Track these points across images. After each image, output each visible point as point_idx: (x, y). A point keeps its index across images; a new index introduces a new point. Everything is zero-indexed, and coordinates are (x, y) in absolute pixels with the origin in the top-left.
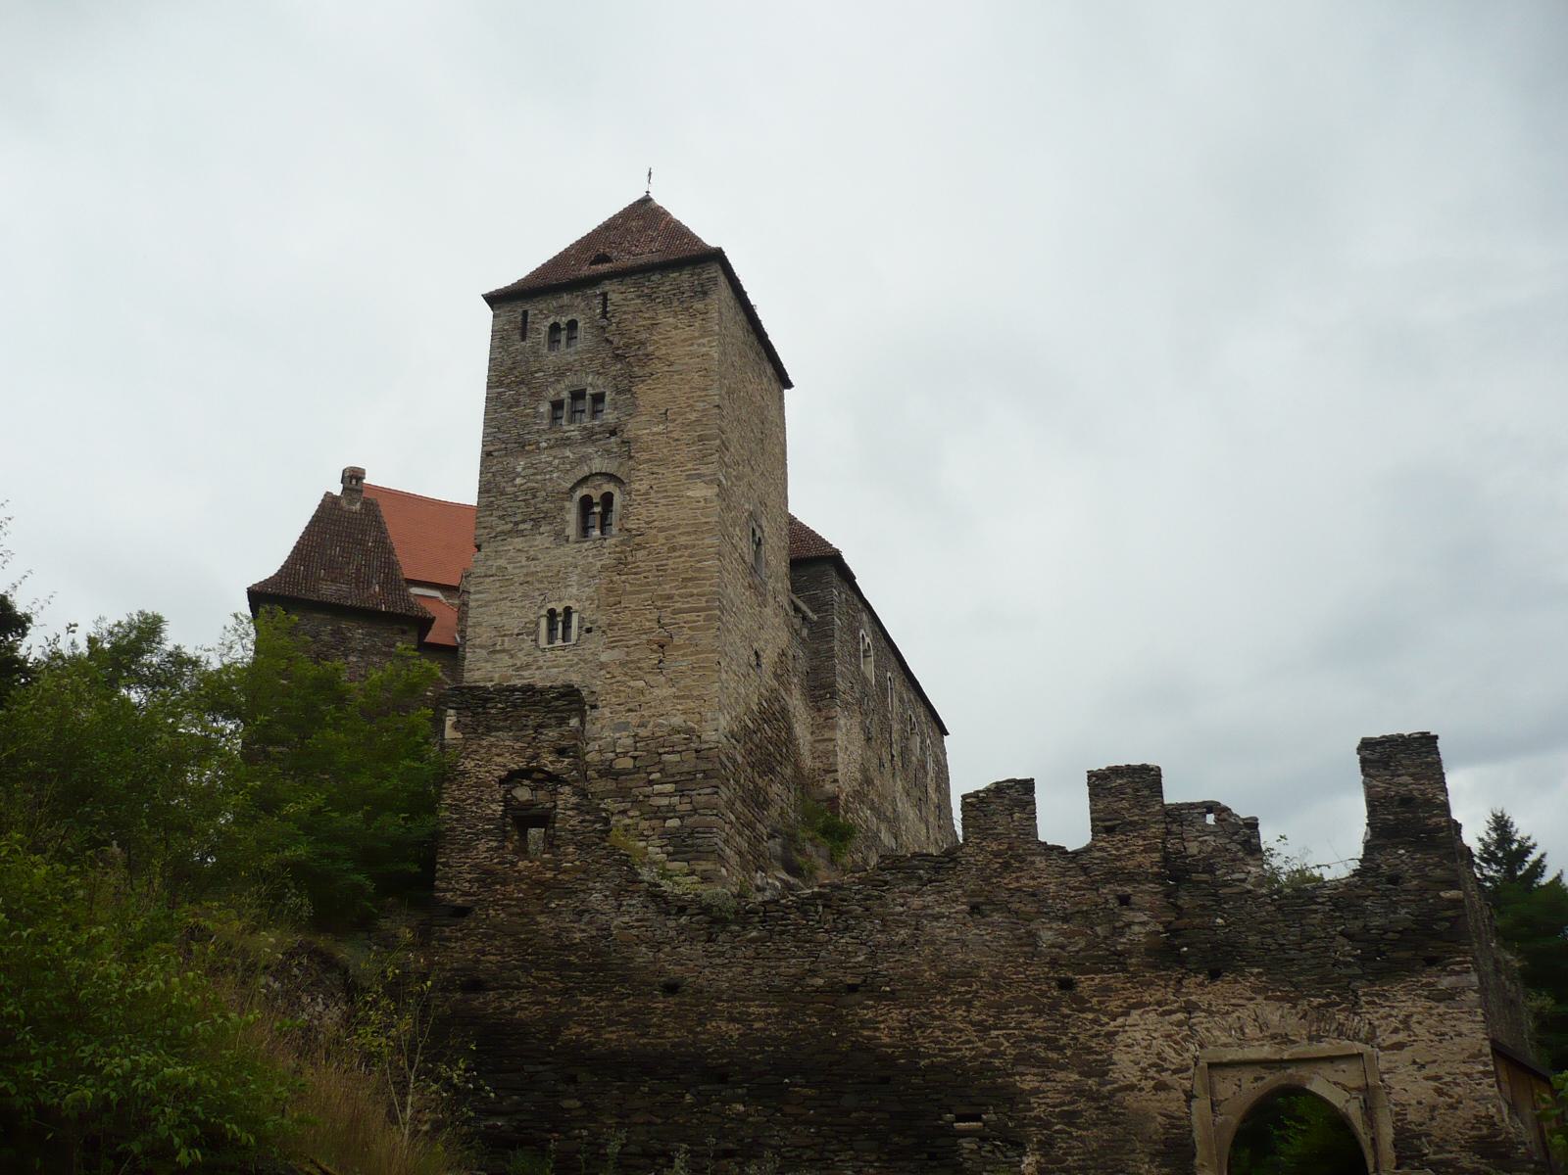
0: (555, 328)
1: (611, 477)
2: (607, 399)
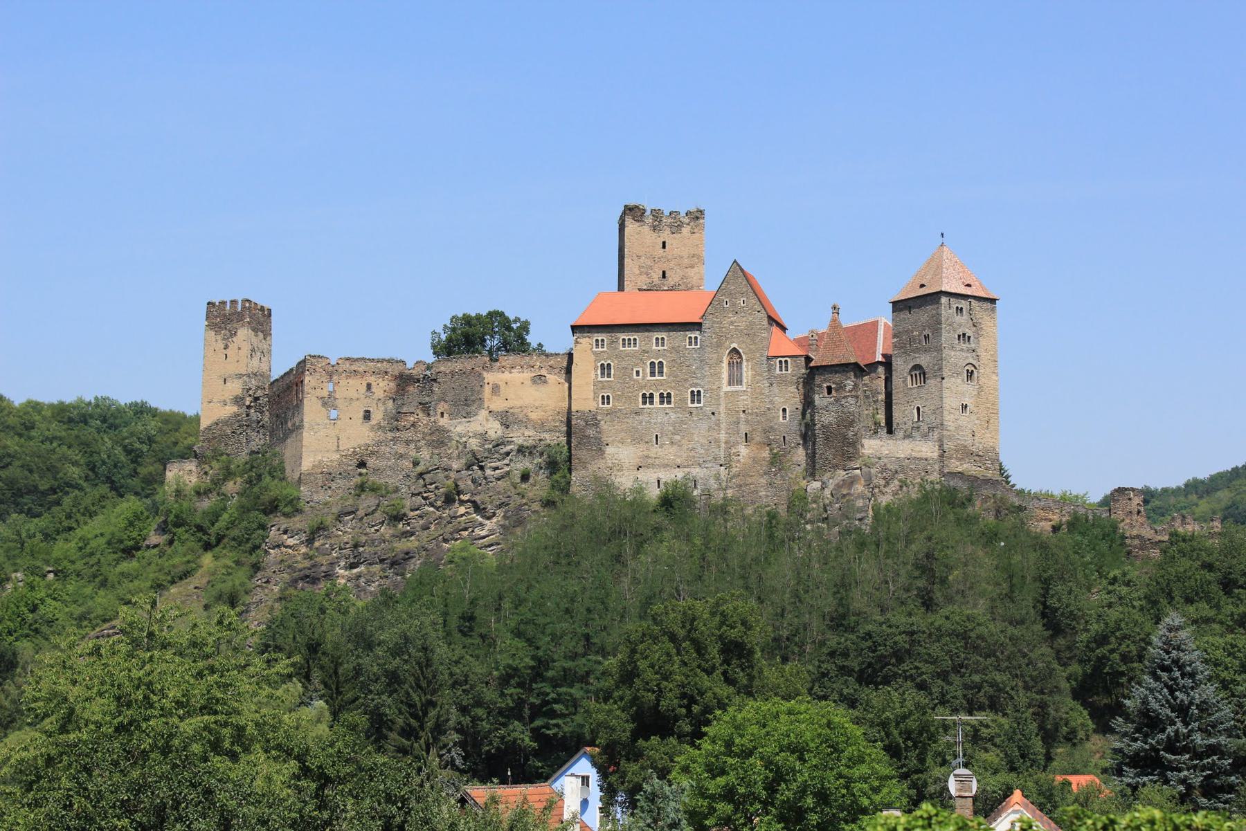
0: (957, 308)
1: (974, 366)
2: (972, 339)
